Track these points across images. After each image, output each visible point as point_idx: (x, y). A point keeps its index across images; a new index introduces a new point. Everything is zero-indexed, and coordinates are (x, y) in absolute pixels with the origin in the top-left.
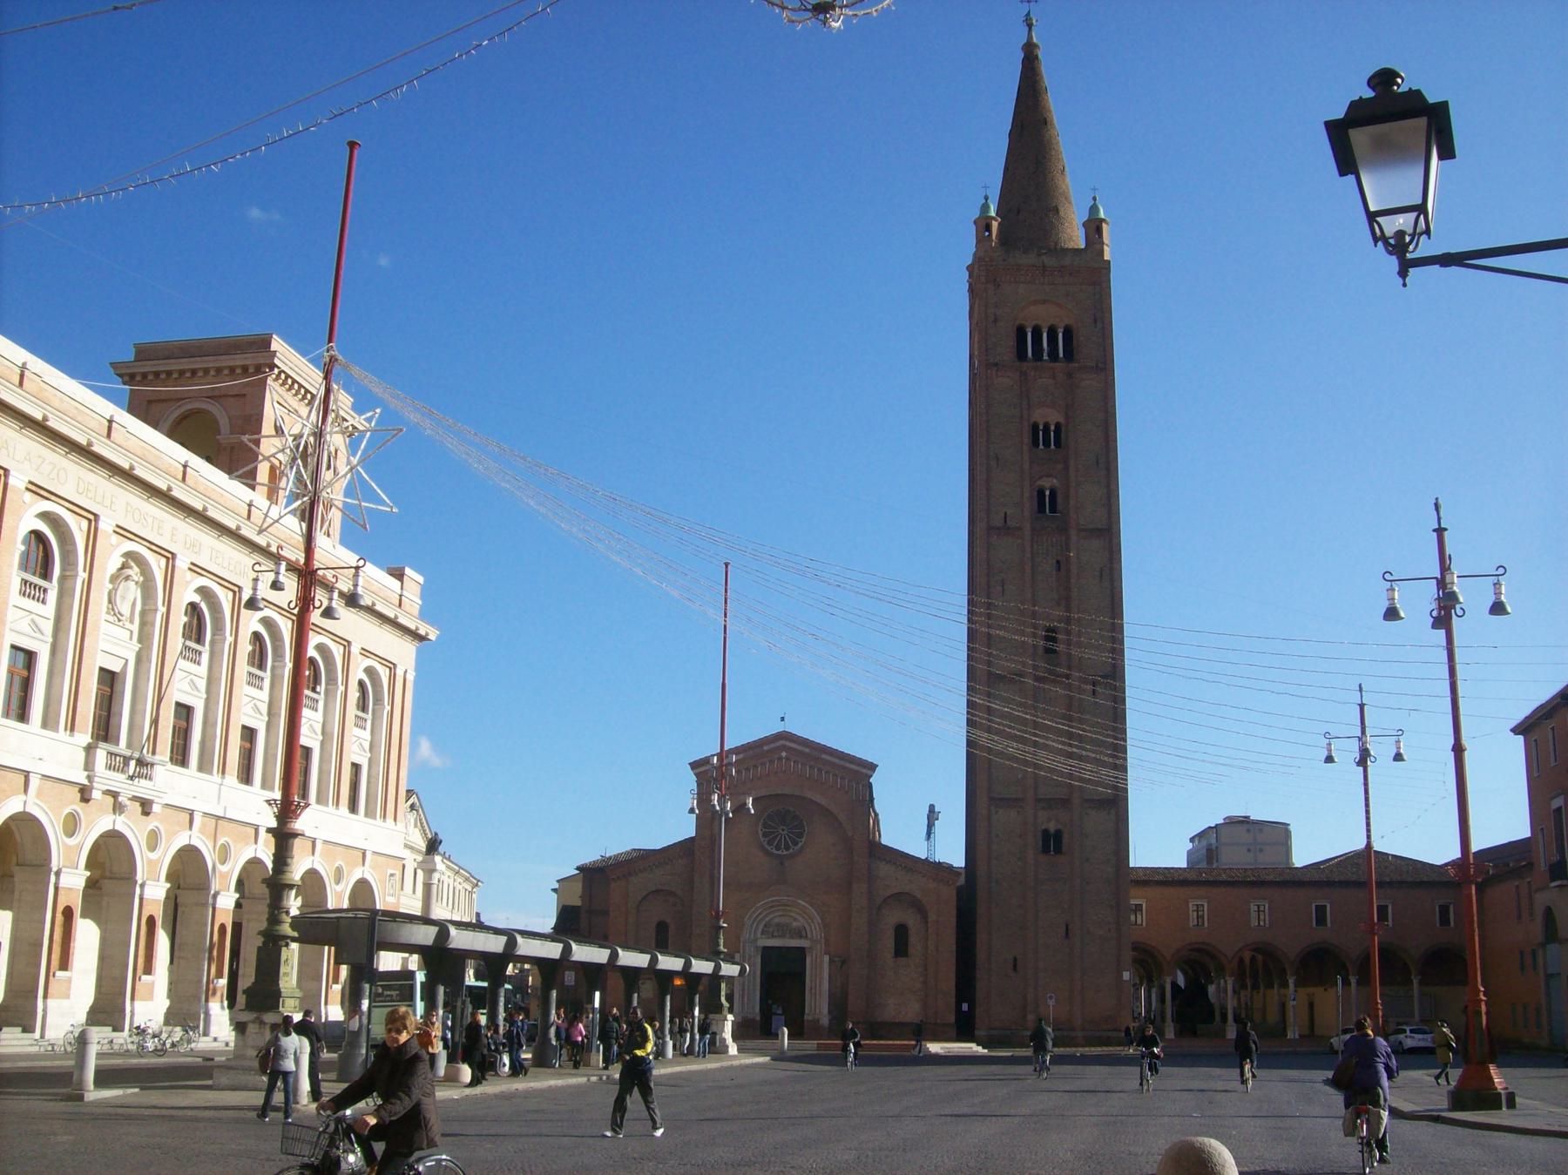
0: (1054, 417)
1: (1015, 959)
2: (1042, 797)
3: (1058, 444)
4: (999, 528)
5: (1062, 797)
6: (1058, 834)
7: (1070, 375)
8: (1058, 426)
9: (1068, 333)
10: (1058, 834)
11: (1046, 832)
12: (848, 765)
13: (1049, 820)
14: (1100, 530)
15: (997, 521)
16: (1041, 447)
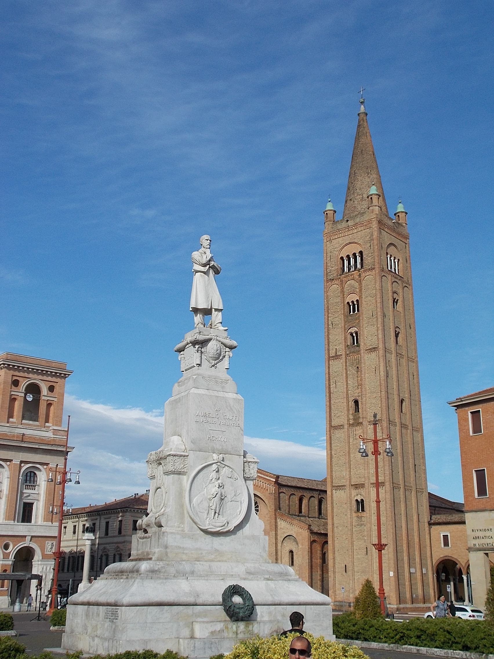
0: (354, 298)
1: (346, 565)
2: (354, 484)
3: (358, 311)
4: (333, 357)
5: (362, 483)
6: (362, 500)
7: (360, 276)
8: (357, 301)
9: (361, 253)
10: (362, 500)
11: (357, 500)
12: (266, 477)
13: (357, 495)
14: (374, 348)
15: (332, 353)
16: (352, 313)
